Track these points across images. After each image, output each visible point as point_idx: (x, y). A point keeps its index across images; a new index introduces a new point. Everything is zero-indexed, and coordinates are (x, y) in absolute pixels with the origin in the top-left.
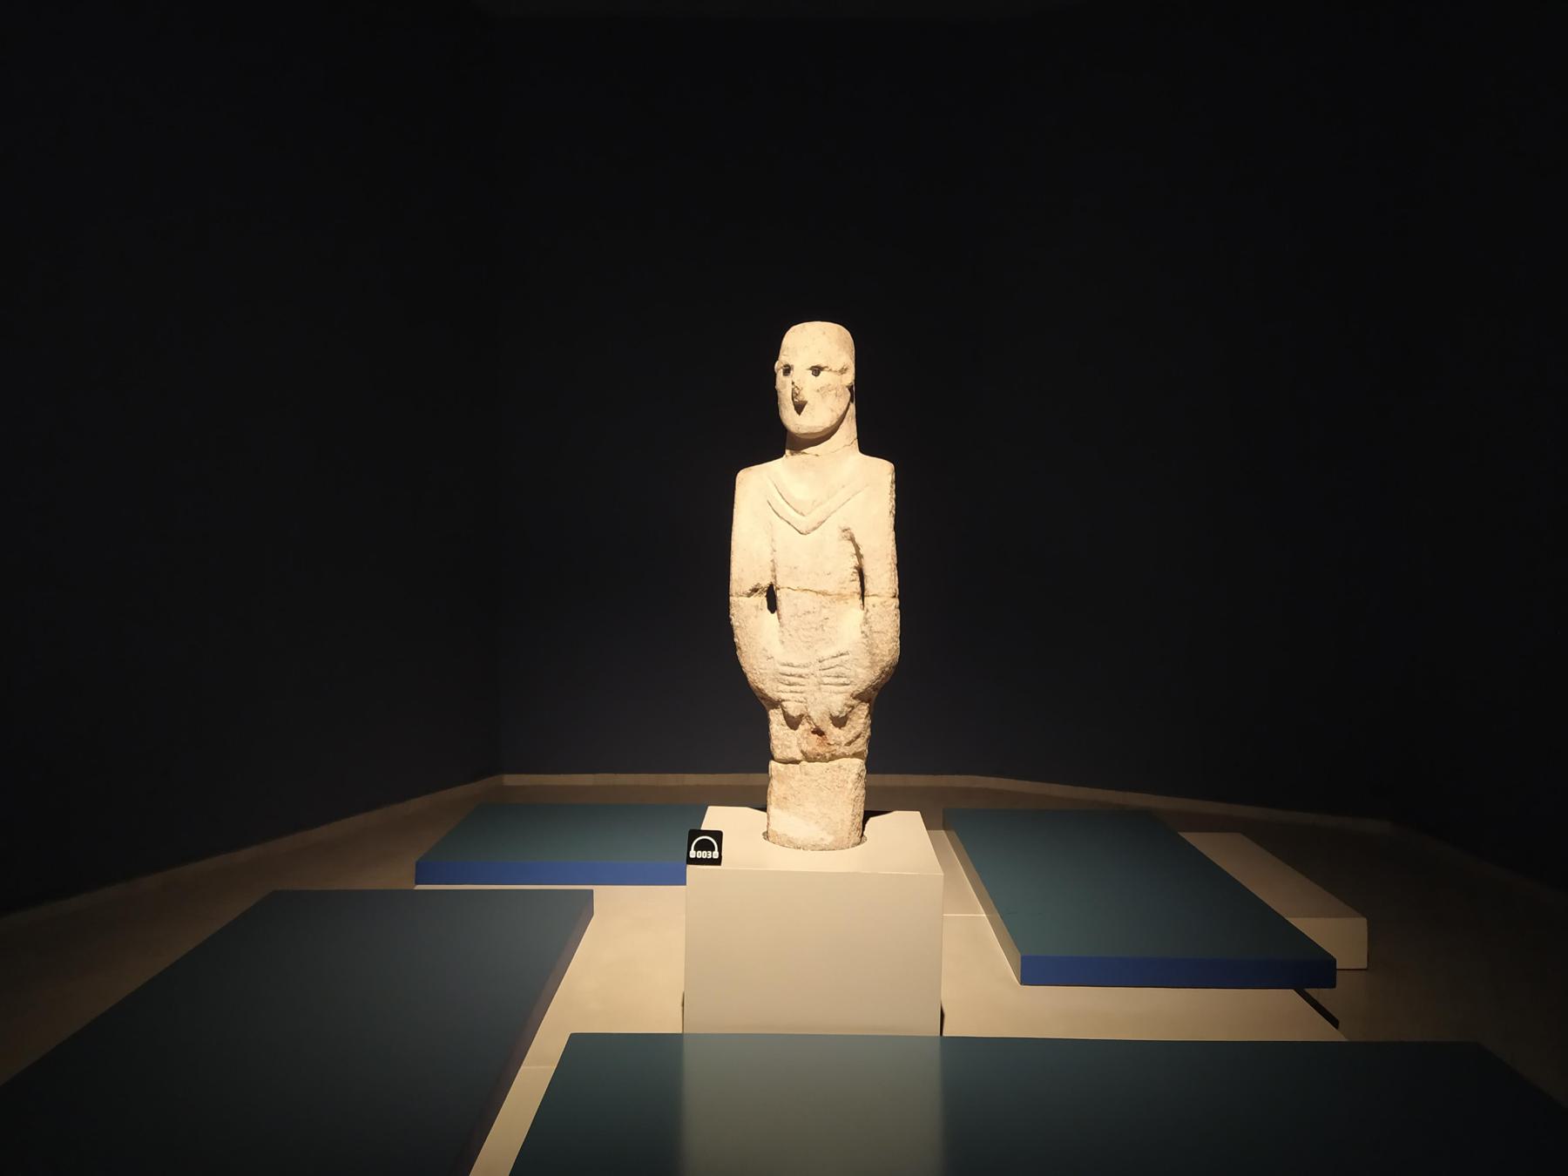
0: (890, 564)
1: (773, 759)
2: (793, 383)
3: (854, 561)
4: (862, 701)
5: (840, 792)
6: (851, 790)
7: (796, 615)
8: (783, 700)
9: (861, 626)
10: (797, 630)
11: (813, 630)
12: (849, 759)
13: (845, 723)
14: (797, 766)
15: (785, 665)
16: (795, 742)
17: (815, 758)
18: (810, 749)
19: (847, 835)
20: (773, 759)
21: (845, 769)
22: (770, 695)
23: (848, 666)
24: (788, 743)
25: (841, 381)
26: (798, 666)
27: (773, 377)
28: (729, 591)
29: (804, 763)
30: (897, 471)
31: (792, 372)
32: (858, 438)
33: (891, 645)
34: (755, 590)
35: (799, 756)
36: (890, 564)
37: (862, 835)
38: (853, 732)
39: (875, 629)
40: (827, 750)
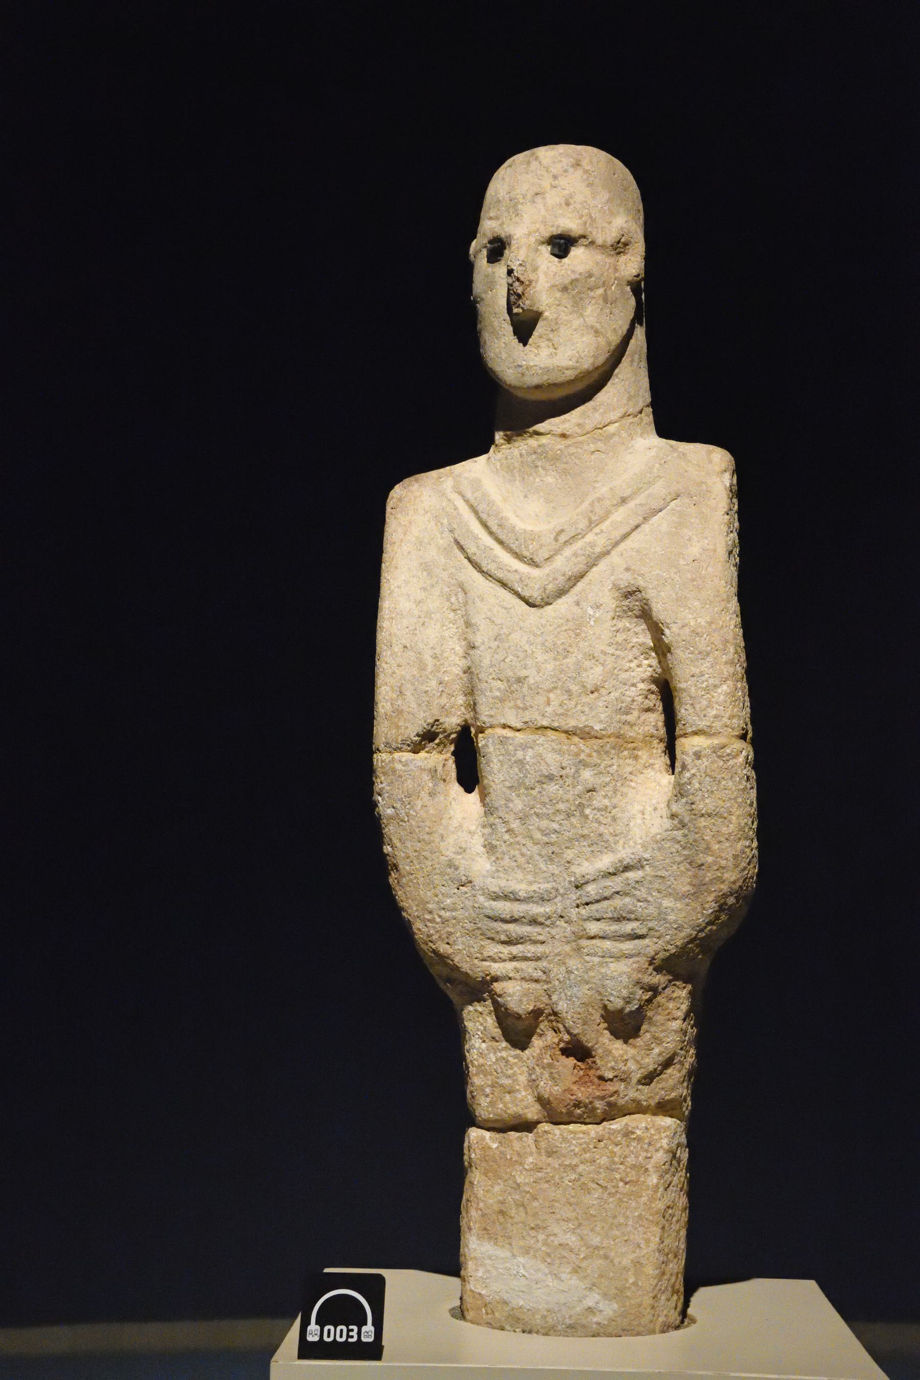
0: (731, 663)
1: (471, 1121)
2: (510, 272)
3: (648, 666)
4: (676, 977)
5: (629, 1195)
6: (657, 1187)
7: (521, 784)
9: (668, 806)
10: (523, 818)
12: (648, 1118)
13: (639, 1029)
14: (529, 1138)
15: (496, 897)
16: (523, 1079)
17: (570, 1113)
19: (647, 1300)
20: (471, 1121)
21: (639, 1139)
22: (465, 967)
23: (642, 893)
24: (506, 1082)
25: (616, 270)
26: (528, 900)
27: (468, 268)
28: (371, 743)
29: (545, 1127)
30: (741, 470)
31: (506, 252)
32: (654, 404)
33: (739, 846)
34: (428, 737)
35: (532, 1112)
36: (731, 663)
37: (684, 1314)
38: (657, 1050)
39: (700, 806)
40: (598, 1093)
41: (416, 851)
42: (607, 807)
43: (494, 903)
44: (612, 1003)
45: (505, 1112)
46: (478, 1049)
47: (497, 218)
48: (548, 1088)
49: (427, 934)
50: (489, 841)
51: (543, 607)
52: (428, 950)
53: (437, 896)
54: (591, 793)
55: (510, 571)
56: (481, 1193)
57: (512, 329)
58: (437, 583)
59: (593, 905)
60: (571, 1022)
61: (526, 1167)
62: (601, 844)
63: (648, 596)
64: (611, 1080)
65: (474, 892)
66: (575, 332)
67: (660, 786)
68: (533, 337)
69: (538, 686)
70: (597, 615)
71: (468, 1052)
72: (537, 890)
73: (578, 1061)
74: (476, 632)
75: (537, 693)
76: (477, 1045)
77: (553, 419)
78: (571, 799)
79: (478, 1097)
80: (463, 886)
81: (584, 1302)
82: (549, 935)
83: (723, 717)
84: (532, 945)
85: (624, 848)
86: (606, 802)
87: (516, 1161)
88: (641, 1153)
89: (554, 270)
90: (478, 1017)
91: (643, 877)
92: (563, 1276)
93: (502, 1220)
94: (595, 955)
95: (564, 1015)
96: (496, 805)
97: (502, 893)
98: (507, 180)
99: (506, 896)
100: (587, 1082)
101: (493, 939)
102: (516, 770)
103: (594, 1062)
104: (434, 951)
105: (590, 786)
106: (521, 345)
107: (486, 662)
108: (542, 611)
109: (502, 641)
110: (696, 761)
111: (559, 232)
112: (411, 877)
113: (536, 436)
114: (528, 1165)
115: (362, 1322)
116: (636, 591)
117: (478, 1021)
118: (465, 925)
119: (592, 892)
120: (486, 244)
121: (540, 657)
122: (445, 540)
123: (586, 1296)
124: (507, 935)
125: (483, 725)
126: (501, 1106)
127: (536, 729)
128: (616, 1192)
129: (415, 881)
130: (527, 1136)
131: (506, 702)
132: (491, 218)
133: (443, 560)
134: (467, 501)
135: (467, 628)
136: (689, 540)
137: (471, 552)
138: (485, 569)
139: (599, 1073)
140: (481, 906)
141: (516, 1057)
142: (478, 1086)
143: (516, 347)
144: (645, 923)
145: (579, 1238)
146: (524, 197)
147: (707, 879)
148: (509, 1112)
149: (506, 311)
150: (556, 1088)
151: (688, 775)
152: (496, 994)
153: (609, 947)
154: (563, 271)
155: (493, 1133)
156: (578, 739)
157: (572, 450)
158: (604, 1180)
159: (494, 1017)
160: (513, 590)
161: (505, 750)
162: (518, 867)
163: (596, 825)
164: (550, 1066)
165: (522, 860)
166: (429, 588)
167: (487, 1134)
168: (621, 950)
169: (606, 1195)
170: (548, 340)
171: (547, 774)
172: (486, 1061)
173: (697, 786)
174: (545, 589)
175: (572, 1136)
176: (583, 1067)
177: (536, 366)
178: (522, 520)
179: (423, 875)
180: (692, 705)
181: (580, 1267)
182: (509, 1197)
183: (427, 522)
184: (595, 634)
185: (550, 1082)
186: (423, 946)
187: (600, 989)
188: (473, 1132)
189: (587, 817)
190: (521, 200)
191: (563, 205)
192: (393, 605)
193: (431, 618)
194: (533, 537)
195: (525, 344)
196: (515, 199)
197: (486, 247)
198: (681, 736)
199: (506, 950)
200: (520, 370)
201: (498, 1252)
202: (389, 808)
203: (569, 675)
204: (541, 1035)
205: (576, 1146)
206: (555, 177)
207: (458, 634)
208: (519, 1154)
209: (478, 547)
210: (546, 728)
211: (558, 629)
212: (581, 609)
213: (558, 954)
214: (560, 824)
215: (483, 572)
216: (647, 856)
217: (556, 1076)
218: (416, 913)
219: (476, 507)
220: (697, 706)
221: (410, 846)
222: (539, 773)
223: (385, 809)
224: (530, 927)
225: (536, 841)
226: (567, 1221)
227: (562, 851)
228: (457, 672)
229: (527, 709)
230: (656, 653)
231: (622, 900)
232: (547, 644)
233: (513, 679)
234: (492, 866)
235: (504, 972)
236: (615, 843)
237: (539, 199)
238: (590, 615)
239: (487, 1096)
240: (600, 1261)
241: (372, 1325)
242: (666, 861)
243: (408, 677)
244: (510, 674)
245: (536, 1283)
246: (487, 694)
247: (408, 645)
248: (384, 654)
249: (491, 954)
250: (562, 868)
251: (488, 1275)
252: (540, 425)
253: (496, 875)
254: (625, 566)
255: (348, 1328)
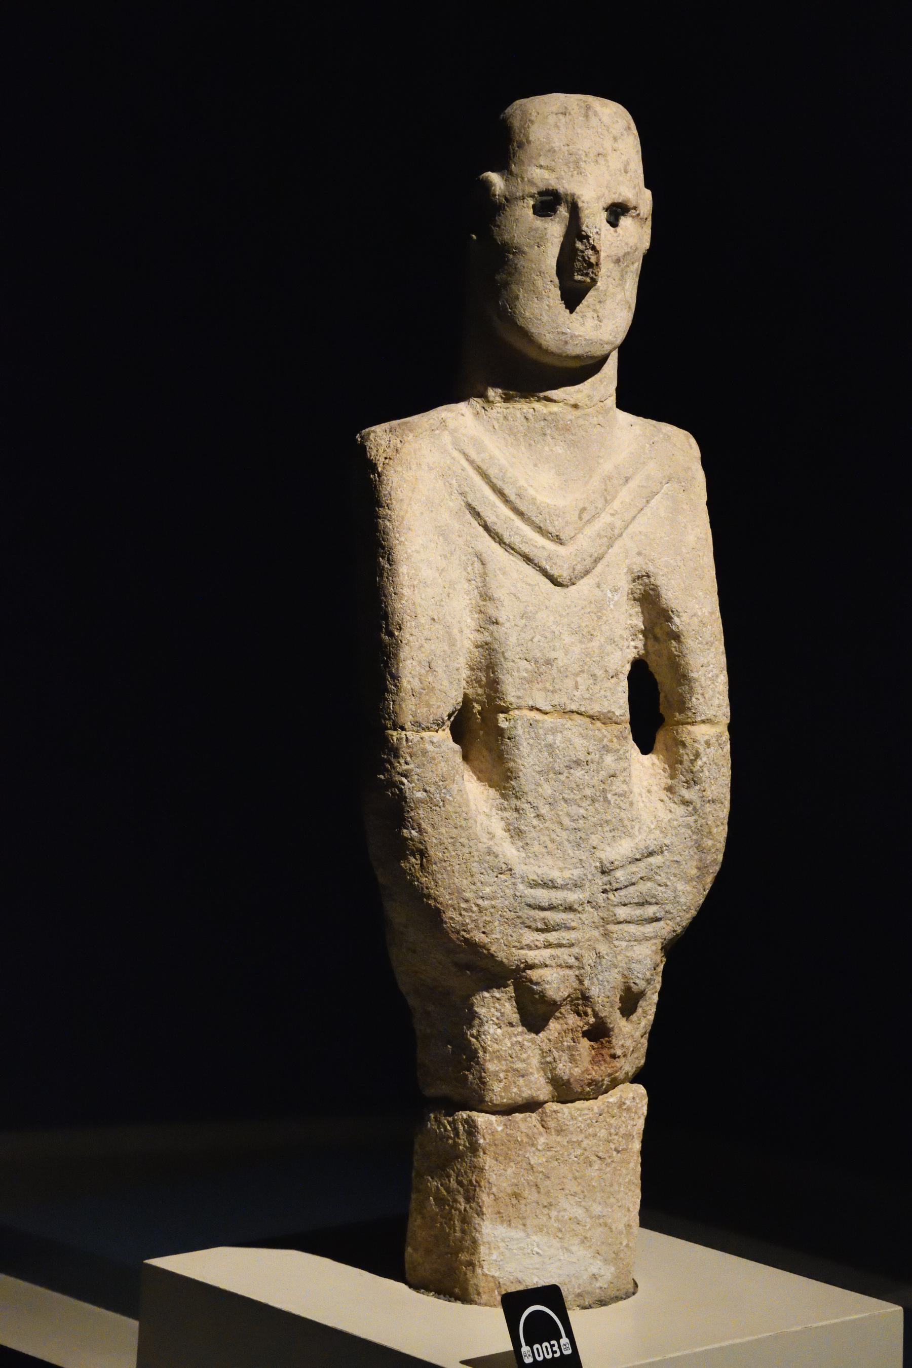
8: (531, 967)
11: (585, 804)
14: (533, 1117)
15: (534, 885)
16: (535, 1061)
18: (577, 1071)
21: (628, 1110)
22: (501, 956)
24: (519, 1065)
29: (556, 1106)
39: (709, 794)
41: (452, 838)
42: (626, 792)
43: (532, 891)
44: (638, 986)
45: (520, 1096)
46: (493, 1035)
47: (551, 169)
48: (567, 1071)
49: (462, 924)
50: (516, 826)
51: (567, 586)
52: (458, 939)
53: (474, 884)
54: (612, 778)
55: (536, 546)
56: (493, 1178)
57: (559, 293)
58: (455, 550)
59: (621, 891)
60: (601, 1007)
61: (540, 1148)
62: (620, 829)
63: (658, 583)
64: (619, 1057)
65: (513, 880)
66: (617, 307)
67: (644, 767)
68: (581, 305)
69: (567, 669)
70: (616, 598)
71: (477, 1038)
72: (571, 877)
73: (590, 1040)
74: (500, 608)
75: (566, 677)
76: (491, 1031)
77: (568, 388)
78: (596, 784)
79: (491, 1082)
80: (501, 874)
81: (589, 1270)
82: (580, 921)
83: (722, 706)
84: (566, 932)
85: (640, 833)
86: (625, 787)
87: (526, 1143)
88: (629, 1122)
89: (610, 239)
90: (494, 1003)
91: (664, 863)
92: (574, 1249)
93: (514, 1201)
94: (623, 939)
95: (596, 999)
96: (526, 789)
97: (542, 881)
98: (563, 129)
99: (545, 884)
100: (600, 1061)
101: (529, 927)
102: (546, 754)
103: (610, 1042)
104: (466, 940)
105: (612, 772)
106: (568, 311)
107: (513, 640)
108: (566, 590)
109: (528, 618)
110: (707, 750)
111: (620, 201)
112: (444, 864)
113: (544, 401)
114: (541, 1146)
115: (558, 1338)
116: (643, 576)
117: (494, 1007)
118: (505, 914)
119: (622, 879)
120: (535, 193)
121: (567, 639)
122: (457, 503)
123: (591, 1264)
124: (545, 923)
125: (509, 706)
126: (515, 1090)
127: (564, 712)
128: (612, 1161)
129: (449, 869)
130: (530, 1117)
131: (534, 684)
132: (541, 167)
133: (456, 525)
134: (471, 462)
135: (485, 600)
136: (684, 527)
137: (490, 520)
138: (507, 541)
139: (612, 1051)
140: (523, 895)
141: (532, 1041)
142: (492, 1072)
143: (562, 312)
144: (663, 906)
145: (585, 1210)
146: (586, 154)
147: (708, 862)
148: (523, 1095)
149: (555, 272)
150: (576, 1069)
151: (699, 763)
152: (531, 981)
153: (634, 931)
154: (618, 242)
155: (498, 1117)
156: (601, 724)
157: (581, 421)
158: (602, 1152)
159: (514, 1004)
160: (539, 567)
161: (535, 733)
162: (548, 853)
163: (618, 811)
164: (569, 1047)
165: (550, 845)
166: (448, 555)
167: (493, 1118)
168: (644, 934)
169: (603, 1165)
170: (594, 310)
171: (575, 759)
172: (500, 1047)
173: (707, 773)
174: (574, 569)
175: (578, 1112)
176: (596, 1046)
177: (581, 336)
178: (537, 491)
179: (458, 862)
180: (703, 694)
181: (586, 1238)
182: (522, 1179)
183: (434, 481)
184: (614, 618)
185: (570, 1064)
186: (454, 936)
187: (625, 973)
188: (478, 1117)
189: (609, 803)
190: (583, 157)
191: (623, 171)
192: (414, 571)
193: (455, 589)
194: (557, 512)
195: (571, 312)
196: (577, 154)
197: (532, 196)
198: (688, 723)
199: (541, 937)
200: (563, 338)
201: (512, 1234)
202: (419, 791)
203: (594, 660)
204: (558, 1018)
205: (581, 1122)
206: (615, 139)
207: (470, 606)
208: (527, 1135)
209: (497, 516)
210: (573, 712)
211: (582, 611)
212: (602, 591)
213: (589, 940)
214: (587, 810)
215: (505, 543)
216: (667, 842)
217: (578, 1058)
218: (450, 902)
219: (487, 470)
220: (707, 696)
221: (444, 832)
222: (568, 758)
223: (415, 792)
224: (564, 914)
225: (565, 827)
226: (574, 1196)
227: (587, 837)
228: (468, 646)
229: (556, 692)
230: (644, 636)
231: (645, 885)
232: (572, 625)
233: (542, 660)
234: (519, 851)
235: (542, 960)
236: (632, 828)
237: (601, 160)
238: (609, 598)
239: (500, 1082)
240: (601, 1229)
241: (567, 1337)
242: (681, 847)
243: (438, 652)
244: (539, 655)
245: (550, 1259)
246: (513, 673)
247: (436, 618)
248: (408, 625)
249: (528, 942)
250: (588, 854)
251: (502, 1257)
252: (553, 391)
253: (527, 861)
254: (636, 550)
255: (550, 1343)
